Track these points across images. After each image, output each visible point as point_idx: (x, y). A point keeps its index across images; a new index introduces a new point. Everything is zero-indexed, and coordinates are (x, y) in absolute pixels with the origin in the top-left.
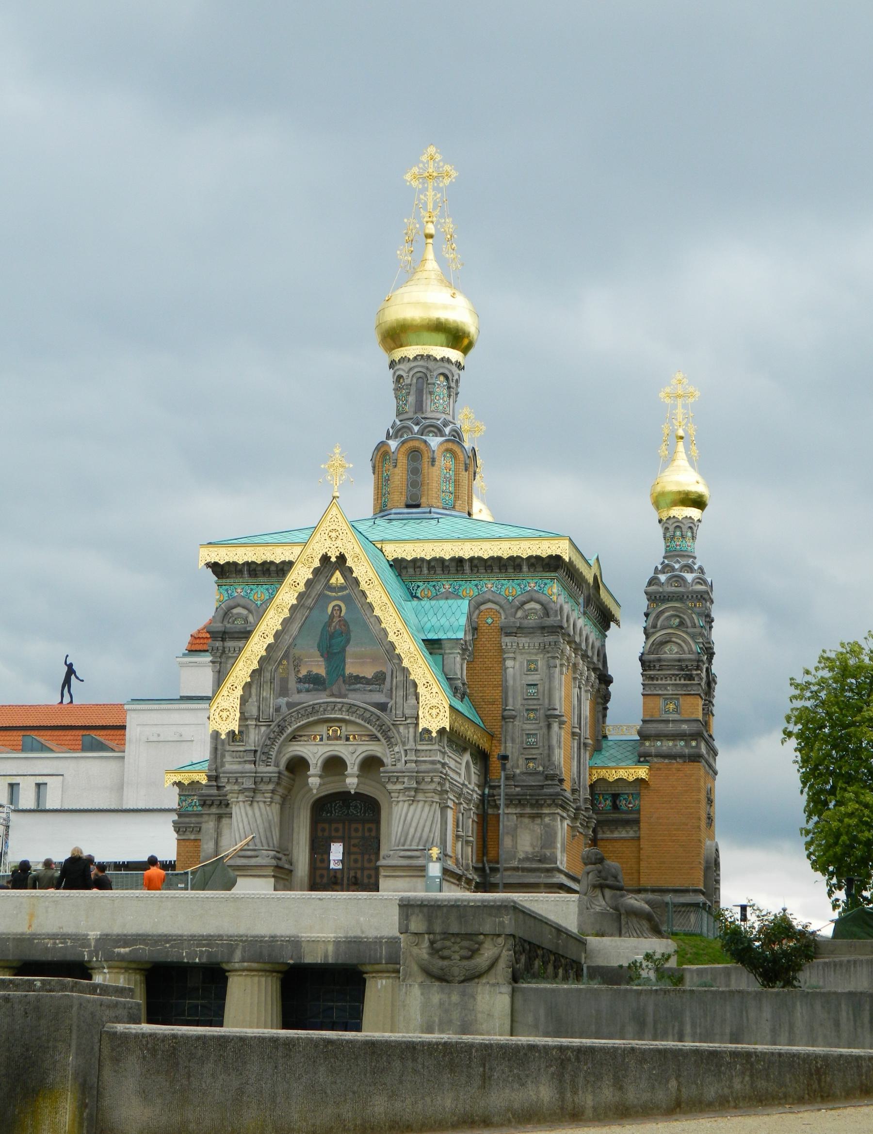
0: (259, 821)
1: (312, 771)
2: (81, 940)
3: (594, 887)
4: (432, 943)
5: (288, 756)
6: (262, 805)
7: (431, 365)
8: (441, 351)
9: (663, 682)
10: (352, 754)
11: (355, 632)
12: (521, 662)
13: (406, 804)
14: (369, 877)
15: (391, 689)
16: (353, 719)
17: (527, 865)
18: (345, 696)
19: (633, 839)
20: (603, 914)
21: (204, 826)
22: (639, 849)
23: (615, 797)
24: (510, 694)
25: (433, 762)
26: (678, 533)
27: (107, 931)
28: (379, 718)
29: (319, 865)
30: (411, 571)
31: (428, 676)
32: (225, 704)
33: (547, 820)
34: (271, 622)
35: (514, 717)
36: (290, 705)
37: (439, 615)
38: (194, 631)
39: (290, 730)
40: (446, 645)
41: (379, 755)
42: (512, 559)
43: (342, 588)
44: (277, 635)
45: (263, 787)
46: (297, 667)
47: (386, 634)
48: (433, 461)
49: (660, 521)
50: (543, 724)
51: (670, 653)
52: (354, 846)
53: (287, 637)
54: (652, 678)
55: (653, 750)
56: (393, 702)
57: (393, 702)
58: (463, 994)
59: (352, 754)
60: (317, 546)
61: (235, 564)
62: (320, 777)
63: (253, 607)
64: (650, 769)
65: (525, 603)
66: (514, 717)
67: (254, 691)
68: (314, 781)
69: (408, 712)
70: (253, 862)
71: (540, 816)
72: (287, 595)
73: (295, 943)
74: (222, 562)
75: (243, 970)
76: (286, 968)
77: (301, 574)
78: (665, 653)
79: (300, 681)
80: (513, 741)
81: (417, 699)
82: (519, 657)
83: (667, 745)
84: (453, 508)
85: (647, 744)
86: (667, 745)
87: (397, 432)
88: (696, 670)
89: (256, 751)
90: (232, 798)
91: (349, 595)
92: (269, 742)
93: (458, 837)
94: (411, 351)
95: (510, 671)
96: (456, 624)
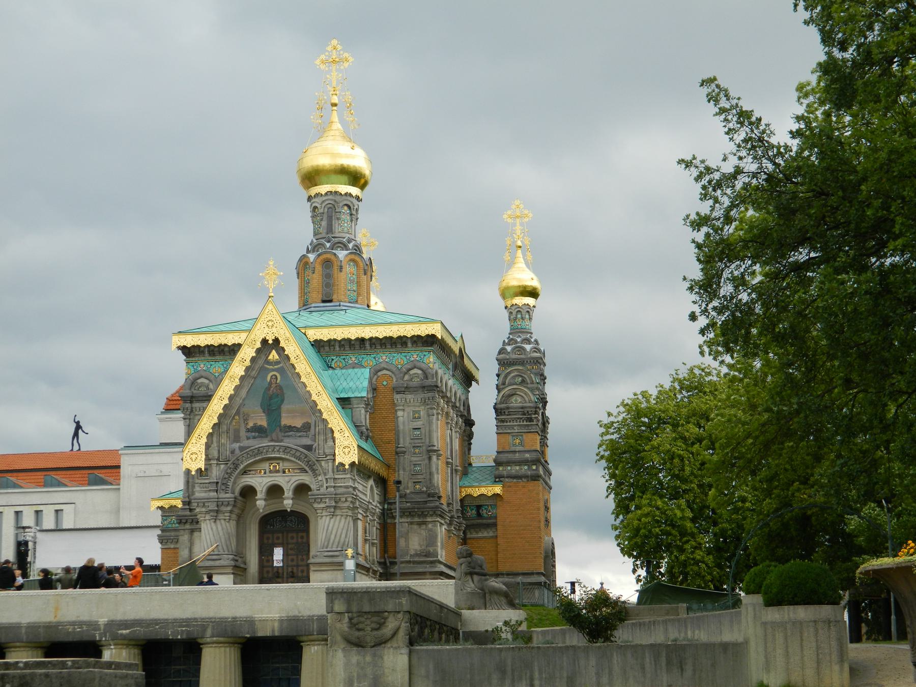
0: (221, 534)
1: (259, 496)
2: (93, 625)
3: (466, 574)
4: (351, 619)
5: (241, 485)
6: (223, 522)
7: (338, 198)
8: (344, 189)
10: (288, 483)
11: (288, 393)
12: (408, 413)
13: (328, 518)
14: (302, 571)
16: (287, 457)
17: (417, 559)
18: (281, 441)
19: (492, 537)
20: (473, 594)
21: (181, 538)
22: (497, 545)
23: (479, 507)
24: (401, 435)
25: (347, 487)
26: (519, 316)
27: (113, 618)
28: (306, 456)
29: (265, 564)
30: (327, 348)
31: (342, 424)
32: (194, 450)
33: (430, 526)
34: (226, 389)
35: (404, 452)
36: (242, 449)
37: (348, 380)
38: (168, 395)
39: (242, 466)
40: (354, 401)
42: (400, 338)
43: (277, 363)
44: (231, 398)
45: (223, 508)
46: (246, 420)
47: (310, 395)
48: (341, 268)
49: (506, 307)
50: (425, 457)
51: (516, 402)
53: (238, 399)
54: (503, 421)
55: (505, 473)
56: (316, 444)
57: (316, 444)
58: (374, 655)
59: (288, 483)
60: (258, 333)
61: (199, 346)
62: (265, 500)
63: (212, 378)
64: (503, 487)
65: (410, 369)
66: (404, 452)
67: (215, 439)
68: (260, 503)
69: (327, 451)
70: (217, 563)
71: (425, 523)
72: (237, 369)
73: (251, 622)
74: (189, 346)
75: (213, 643)
76: (244, 640)
77: (247, 353)
79: (248, 430)
80: (404, 470)
81: (334, 441)
82: (407, 409)
83: (515, 469)
84: (356, 302)
85: (501, 468)
86: (515, 469)
87: (314, 248)
90: (200, 517)
91: (282, 367)
93: (366, 540)
94: (323, 189)
95: (401, 419)
96: (360, 386)
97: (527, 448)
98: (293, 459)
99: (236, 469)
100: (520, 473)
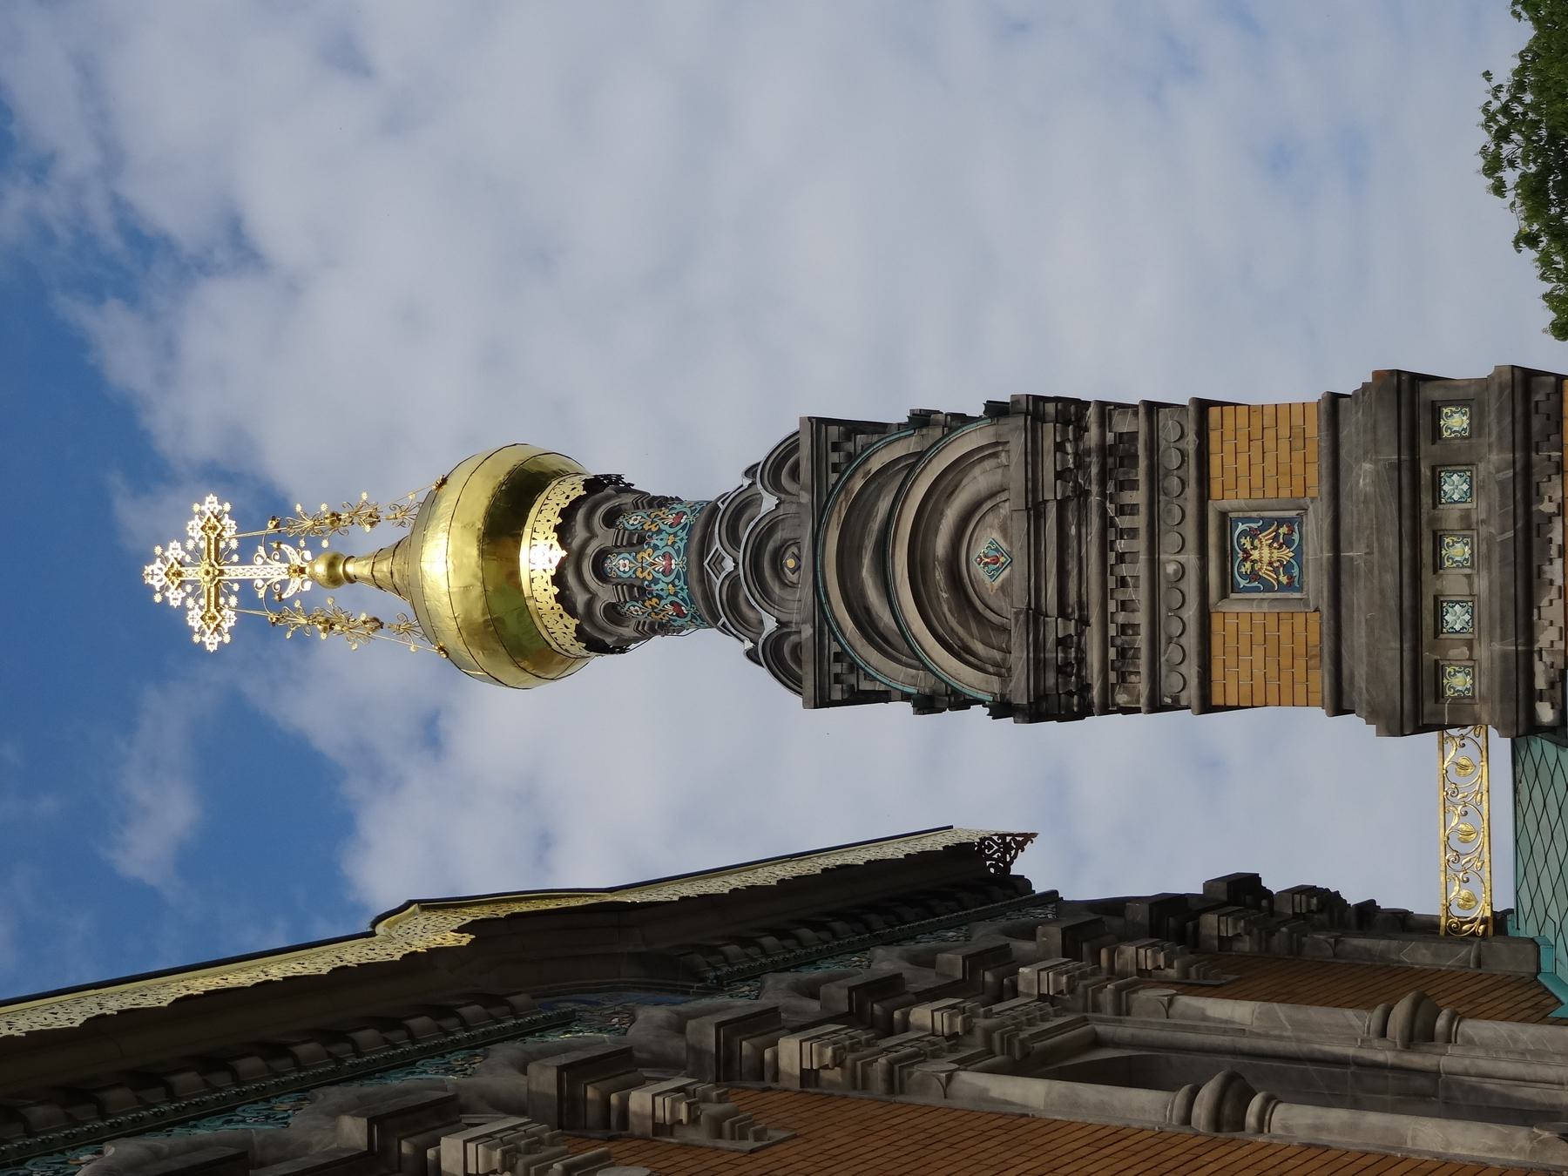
9: (1141, 596)
78: (1004, 589)
83: (1465, 567)
85: (1458, 682)
88: (1081, 429)
97: (1317, 487)
100: (1497, 530)
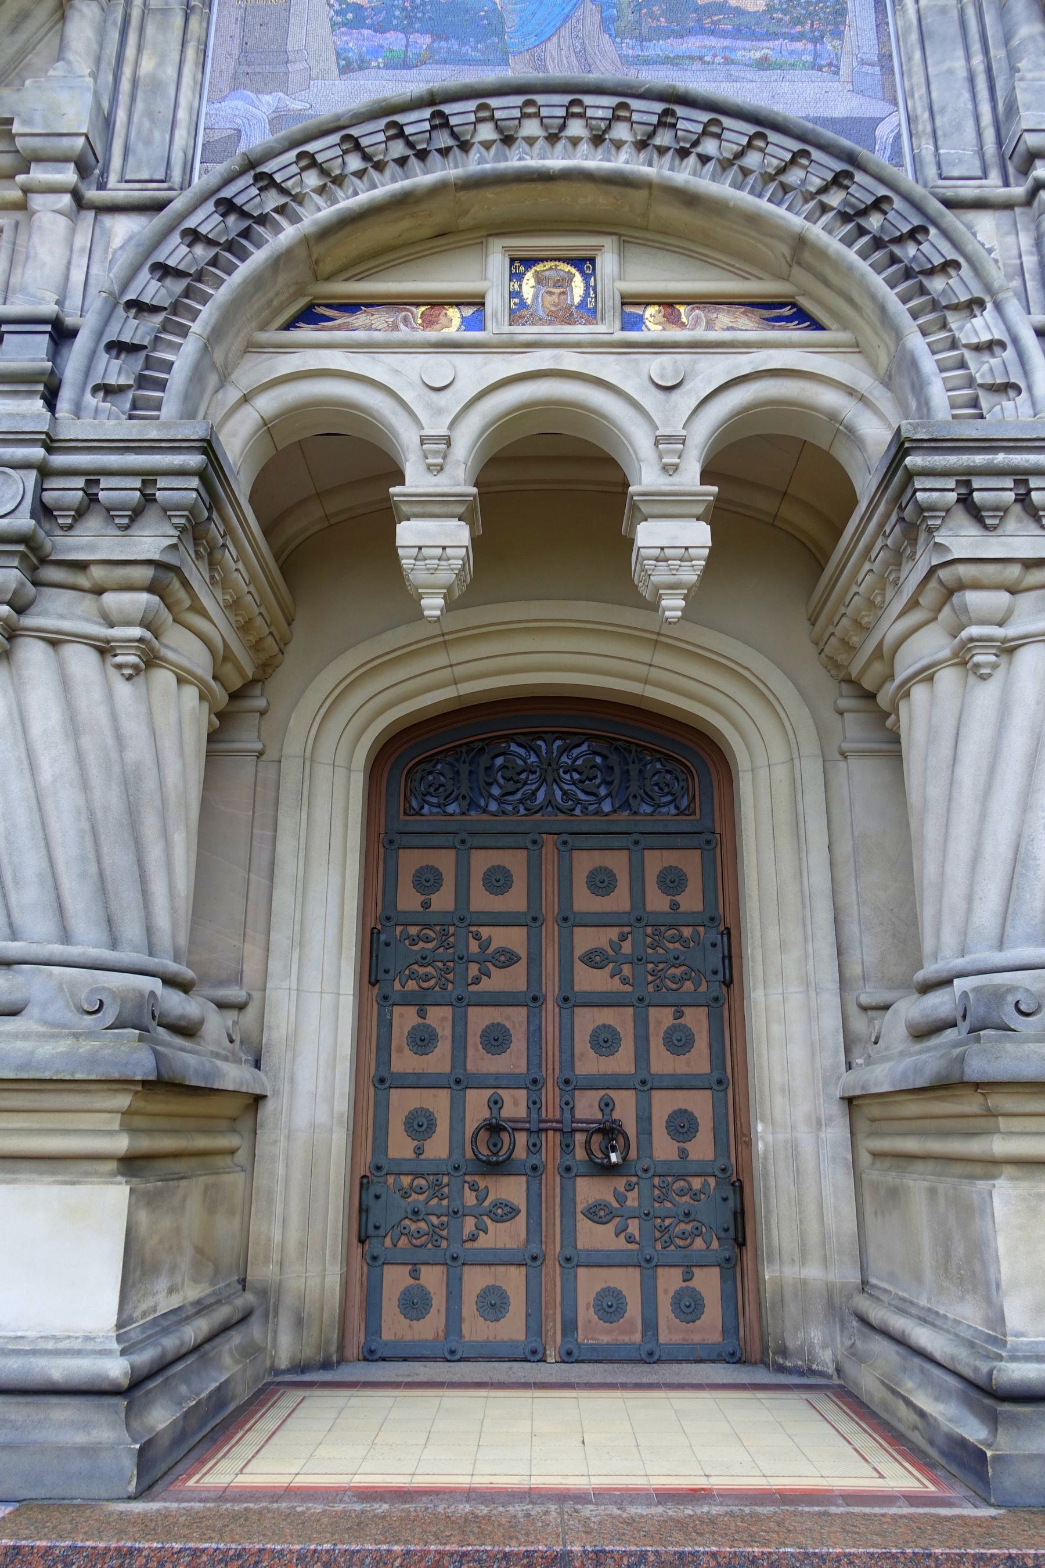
0: (54, 761)
5: (267, 404)
6: (81, 661)
10: (667, 396)
14: (682, 1126)
15: (885, 60)
29: (405, 1061)
39: (289, 233)
41: (828, 398)
45: (92, 541)
52: (594, 959)
59: (667, 396)
89: (61, 334)
92: (150, 289)
98: (722, 189)
99: (234, 249)
